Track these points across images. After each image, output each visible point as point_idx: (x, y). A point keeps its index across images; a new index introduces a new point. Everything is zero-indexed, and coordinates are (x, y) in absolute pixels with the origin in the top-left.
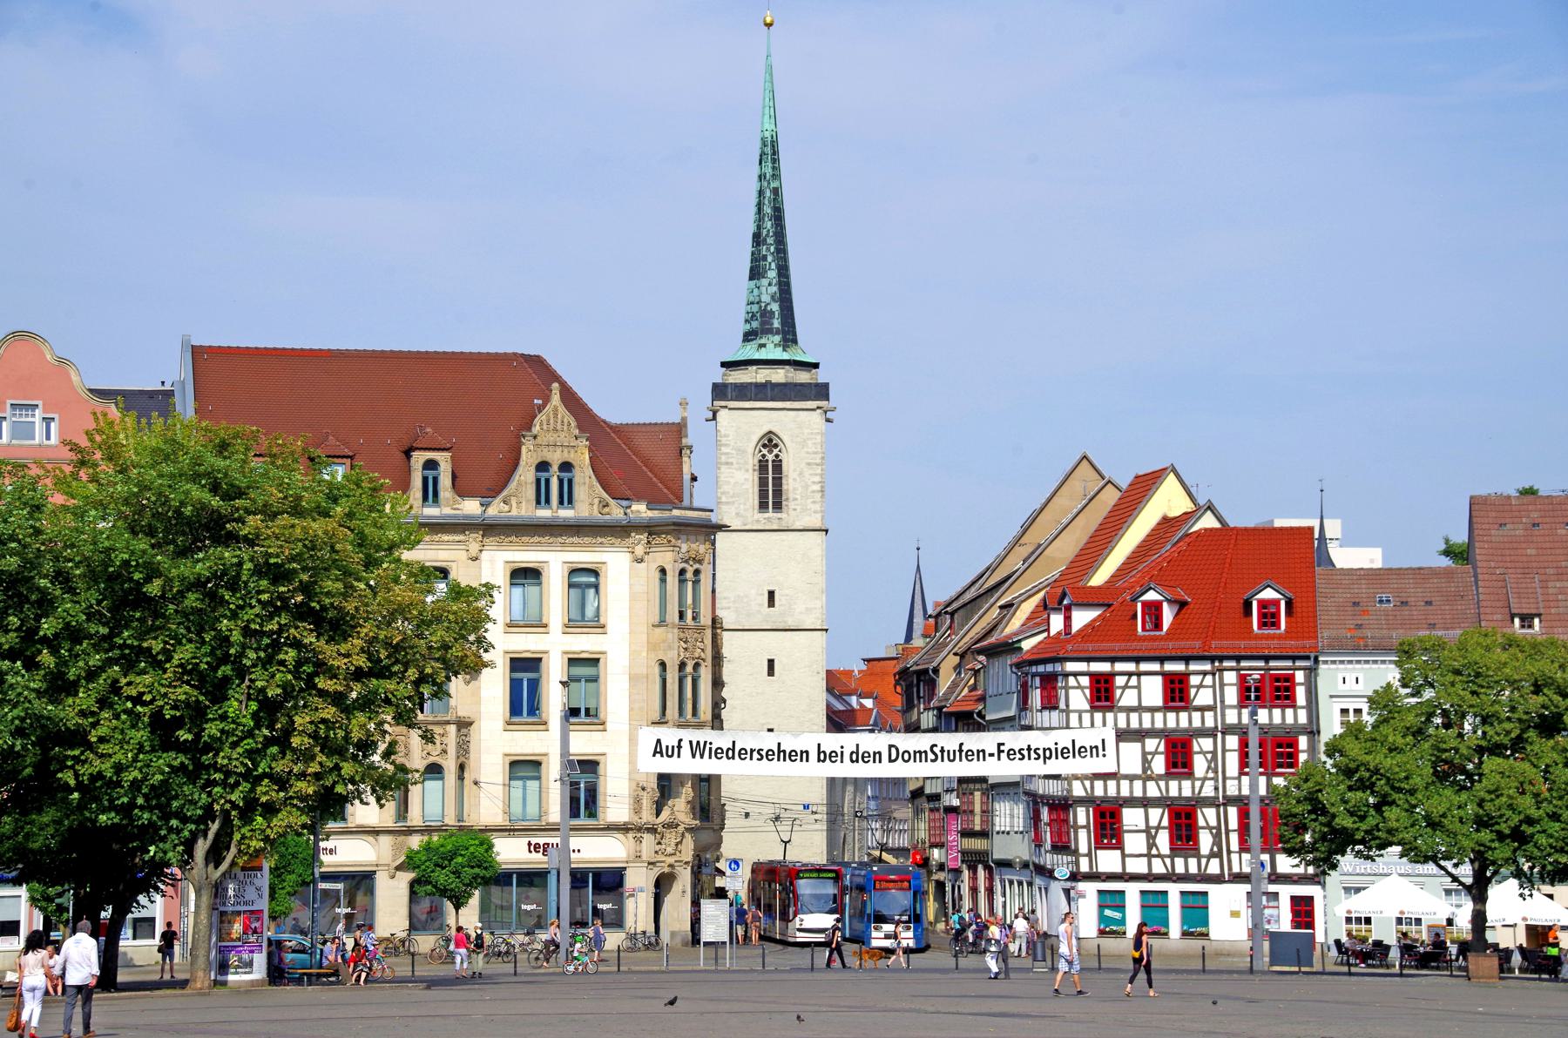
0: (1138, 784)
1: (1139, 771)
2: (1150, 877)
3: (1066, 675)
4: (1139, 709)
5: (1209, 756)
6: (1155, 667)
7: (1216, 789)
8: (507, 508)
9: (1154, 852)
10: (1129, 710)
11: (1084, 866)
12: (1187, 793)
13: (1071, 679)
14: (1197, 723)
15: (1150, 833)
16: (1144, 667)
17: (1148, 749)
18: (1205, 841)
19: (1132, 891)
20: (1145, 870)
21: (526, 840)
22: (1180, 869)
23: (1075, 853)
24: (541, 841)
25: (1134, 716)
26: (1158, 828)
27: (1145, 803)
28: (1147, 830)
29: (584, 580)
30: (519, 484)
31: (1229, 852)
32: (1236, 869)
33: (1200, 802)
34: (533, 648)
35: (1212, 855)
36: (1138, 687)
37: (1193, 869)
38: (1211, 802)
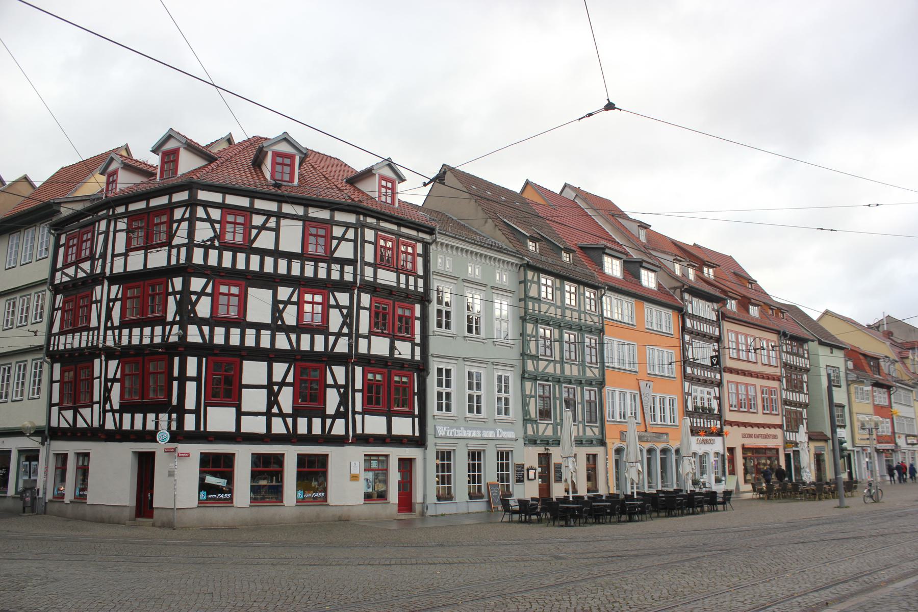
0: (266, 336)
1: (268, 320)
2: (269, 438)
3: (192, 204)
4: (277, 254)
5: (345, 311)
6: (299, 210)
7: (350, 345)
9: (275, 410)
10: (263, 253)
11: (190, 423)
12: (319, 347)
13: (200, 212)
14: (335, 276)
15: (272, 390)
16: (287, 209)
17: (279, 298)
18: (332, 399)
19: (243, 455)
20: (263, 430)
22: (302, 429)
23: (181, 410)
25: (269, 262)
26: (283, 384)
27: (270, 356)
28: (270, 384)
31: (354, 413)
32: (359, 431)
33: (331, 358)
35: (338, 415)
36: (277, 230)
37: (317, 430)
38: (341, 359)
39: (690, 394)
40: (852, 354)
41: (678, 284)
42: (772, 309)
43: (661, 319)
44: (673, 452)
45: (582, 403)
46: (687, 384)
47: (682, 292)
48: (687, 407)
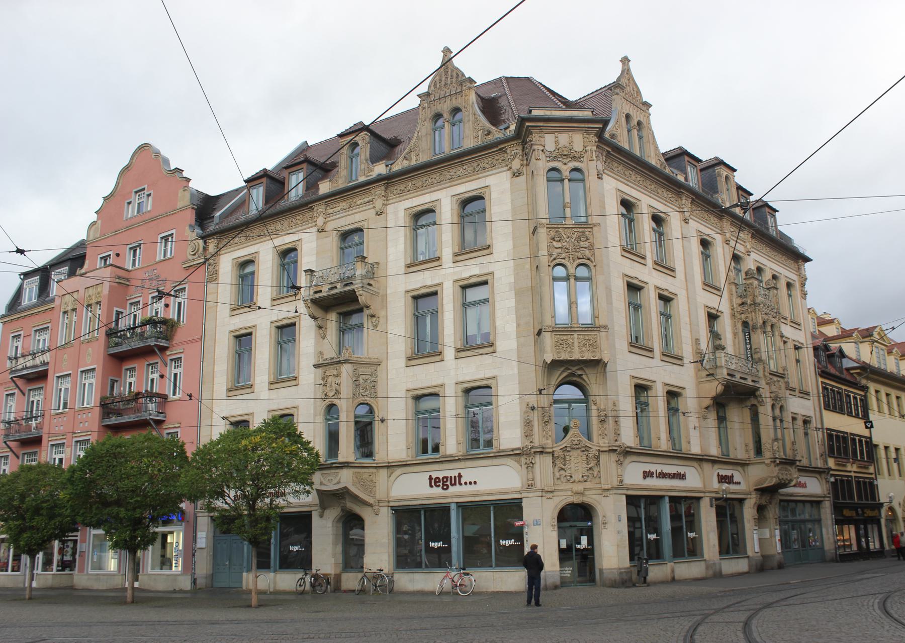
8: (407, 162)
21: (427, 475)
24: (441, 475)
29: (471, 206)
30: (418, 139)
34: (429, 283)
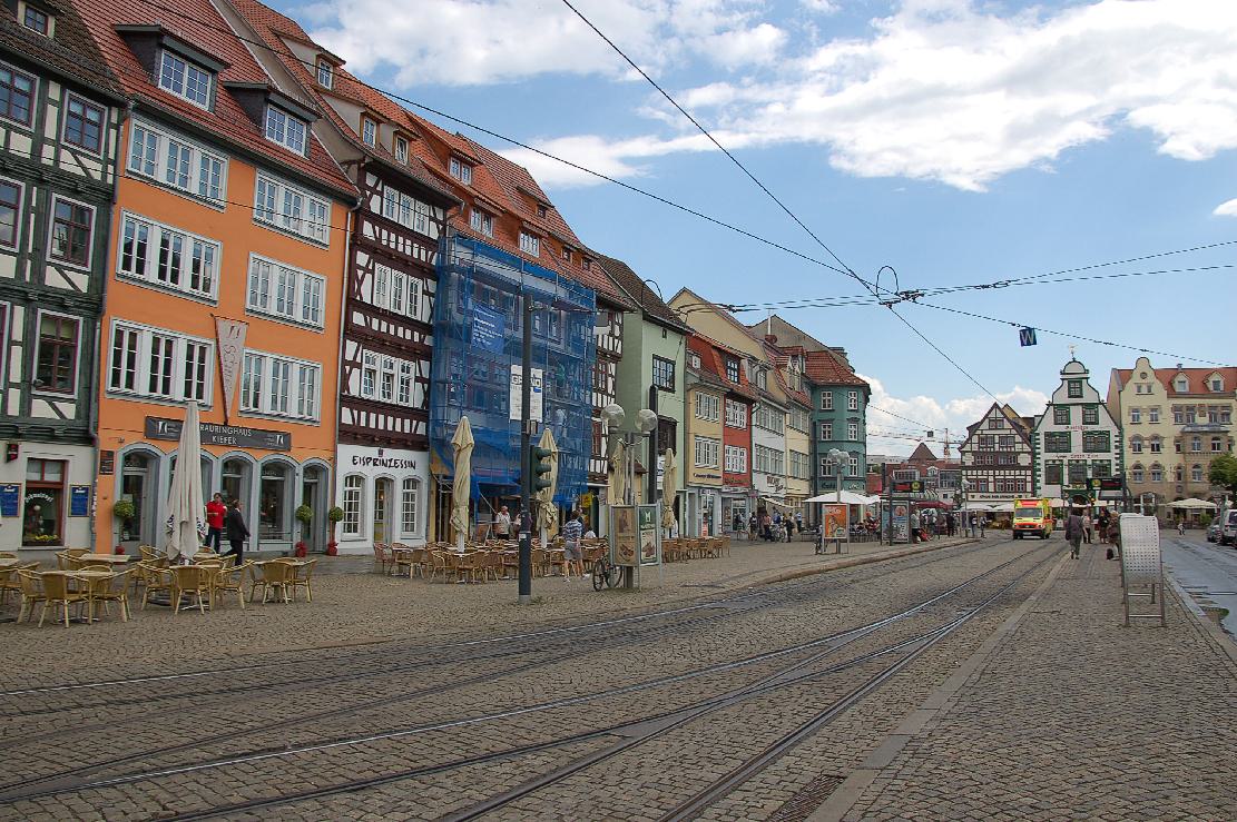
39: (354, 364)
40: (696, 343)
41: (356, 156)
42: (568, 251)
43: (316, 219)
44: (300, 470)
45: (27, 344)
46: (351, 346)
47: (363, 171)
48: (345, 386)
